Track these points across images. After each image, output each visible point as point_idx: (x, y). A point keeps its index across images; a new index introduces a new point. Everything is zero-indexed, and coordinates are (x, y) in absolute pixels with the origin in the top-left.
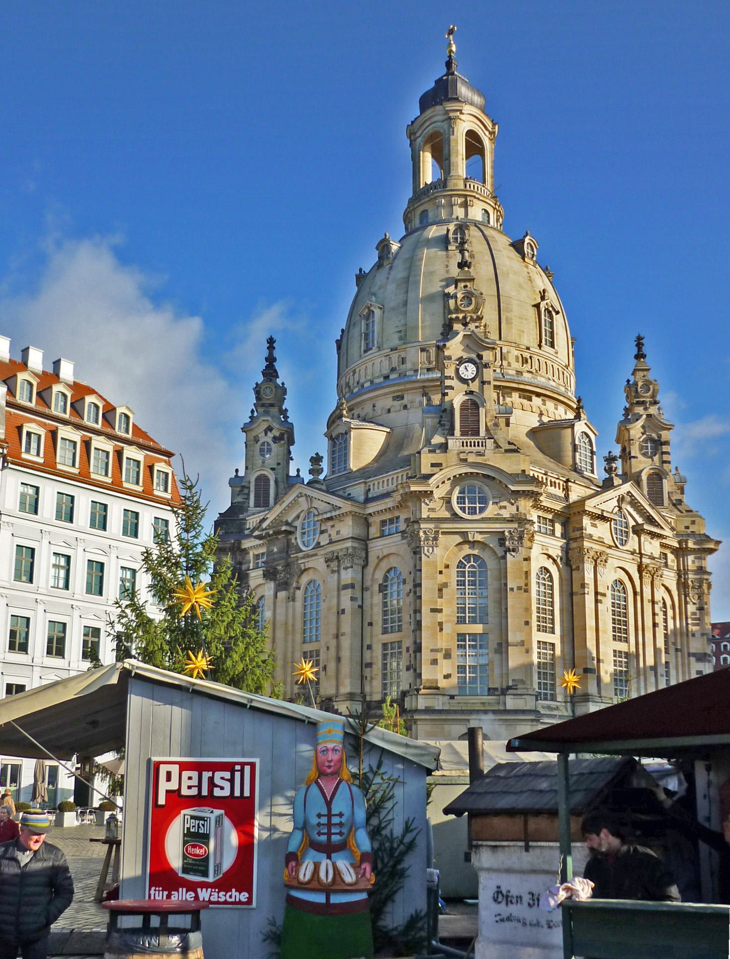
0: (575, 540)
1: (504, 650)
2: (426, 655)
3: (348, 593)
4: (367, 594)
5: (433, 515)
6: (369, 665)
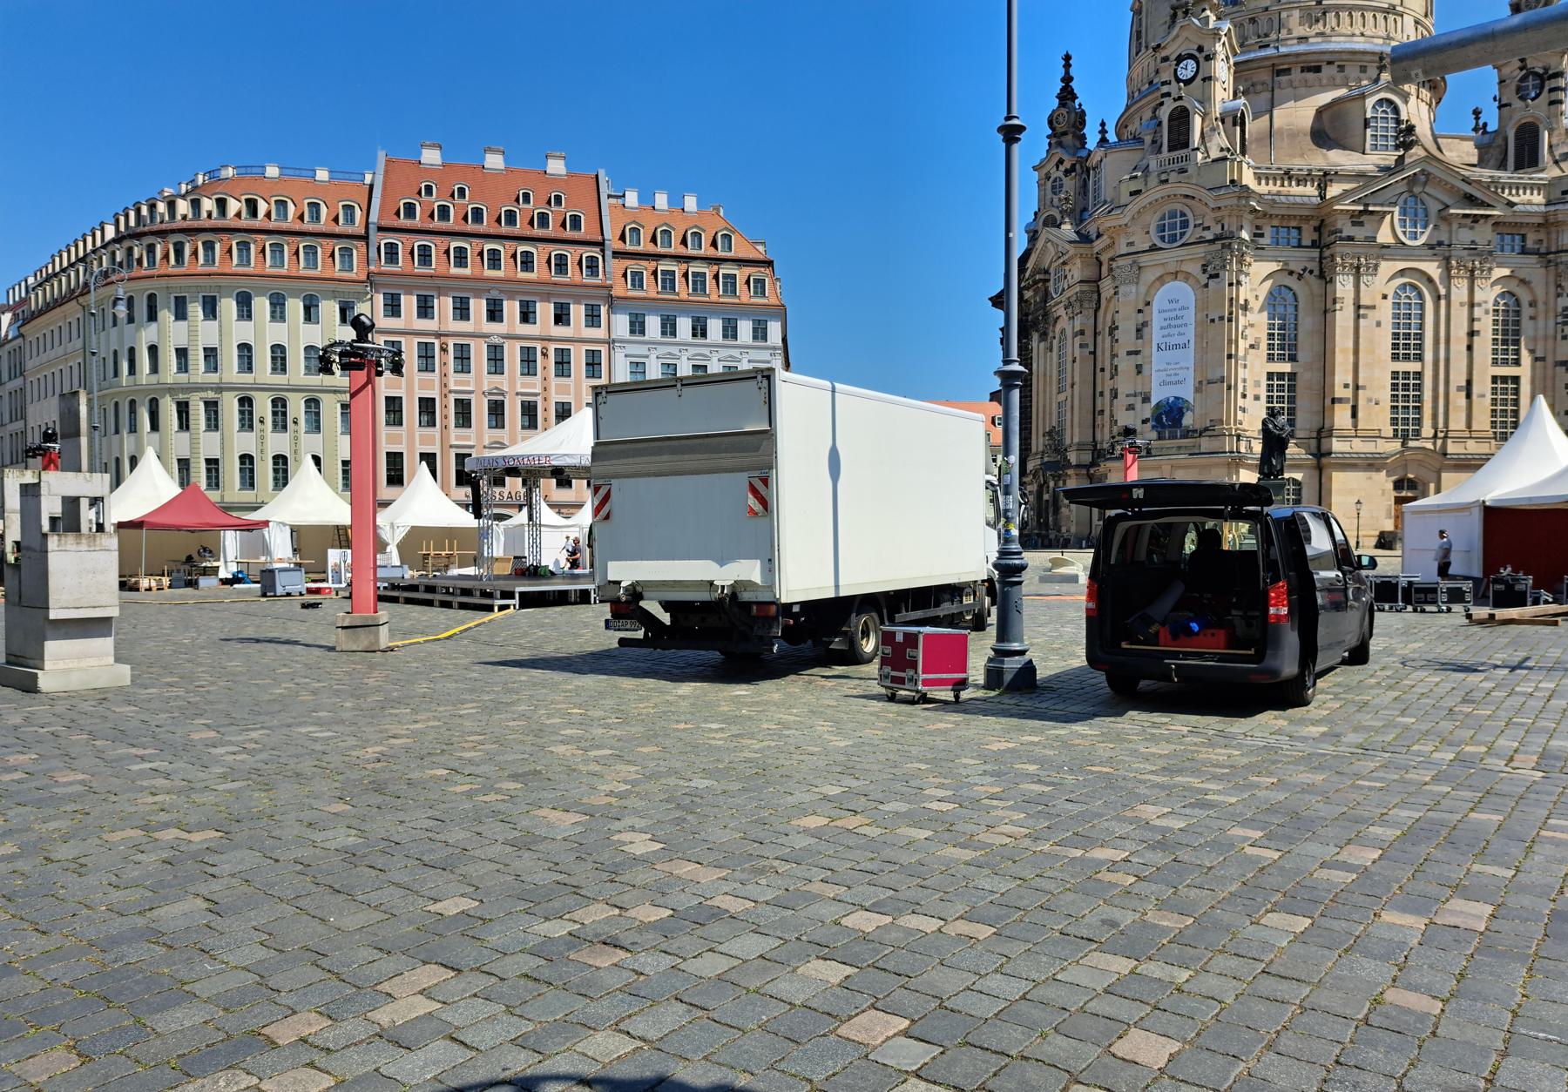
0: (1328, 246)
2: (1122, 401)
3: (1078, 340)
4: (1099, 338)
5: (1132, 249)
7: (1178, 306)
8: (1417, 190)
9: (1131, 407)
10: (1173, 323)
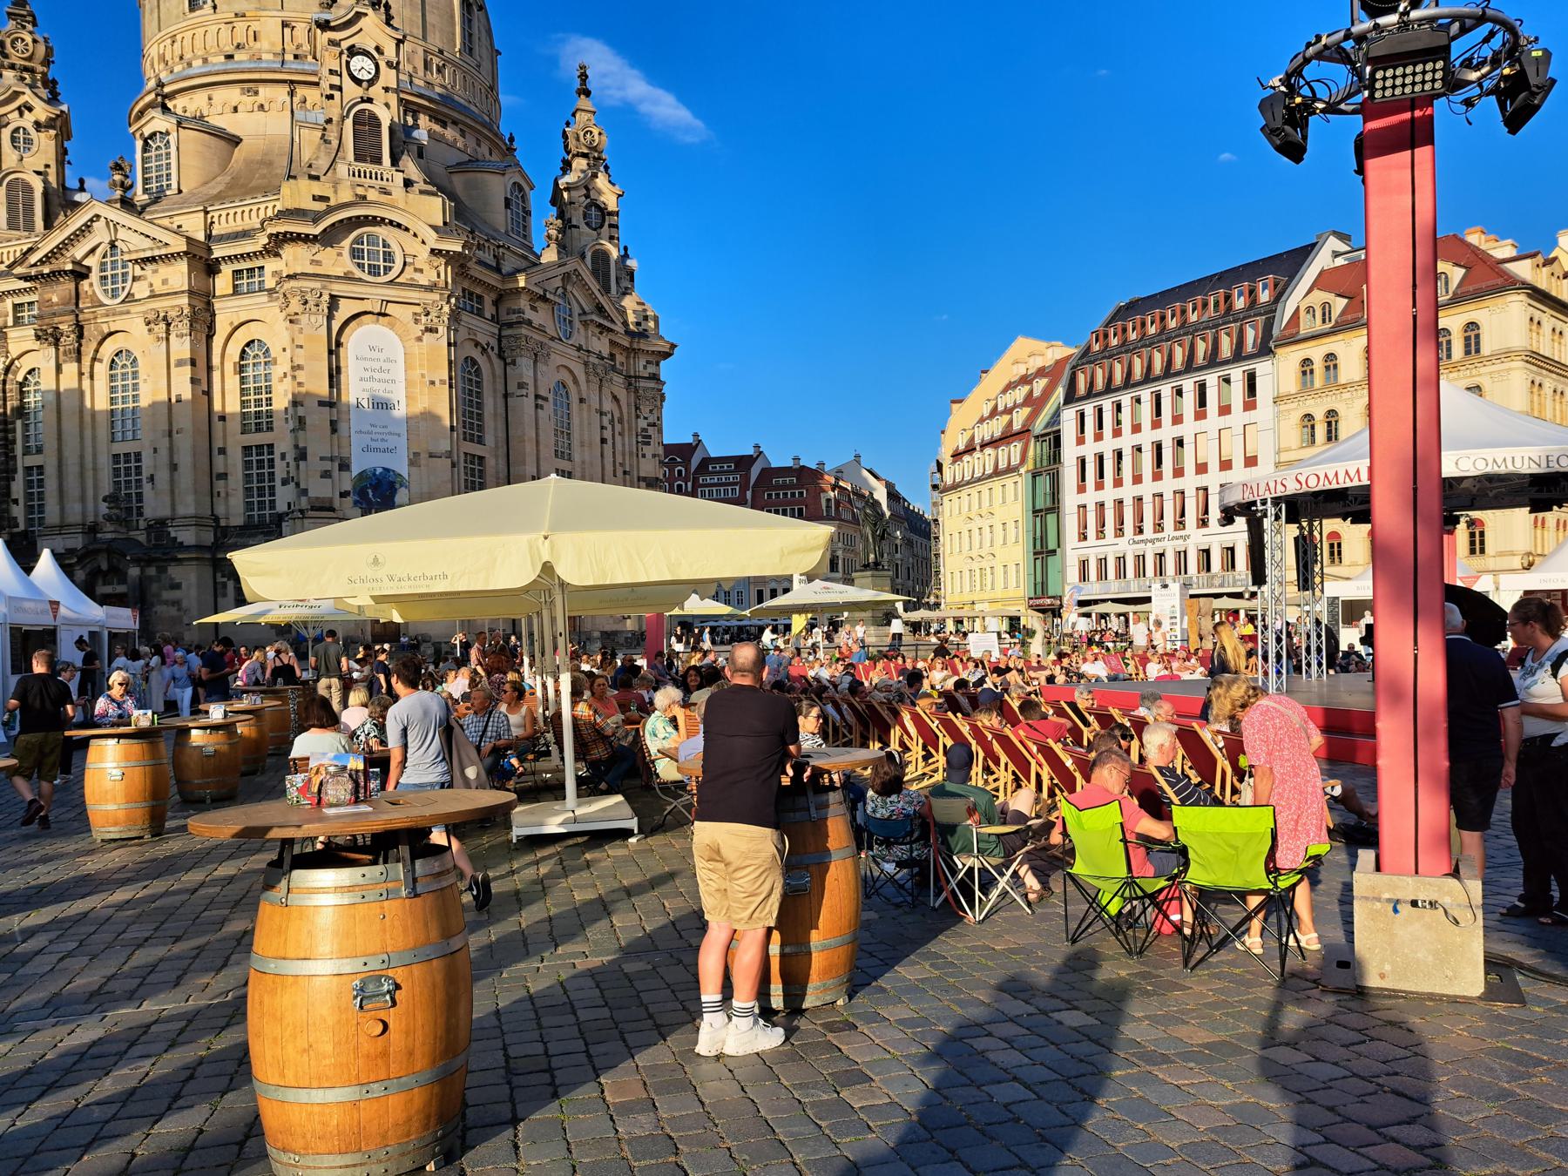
0: (510, 325)
1: (423, 462)
2: (314, 464)
4: (216, 375)
6: (223, 476)
7: (382, 356)
8: (569, 288)
9: (326, 474)
10: (377, 375)
